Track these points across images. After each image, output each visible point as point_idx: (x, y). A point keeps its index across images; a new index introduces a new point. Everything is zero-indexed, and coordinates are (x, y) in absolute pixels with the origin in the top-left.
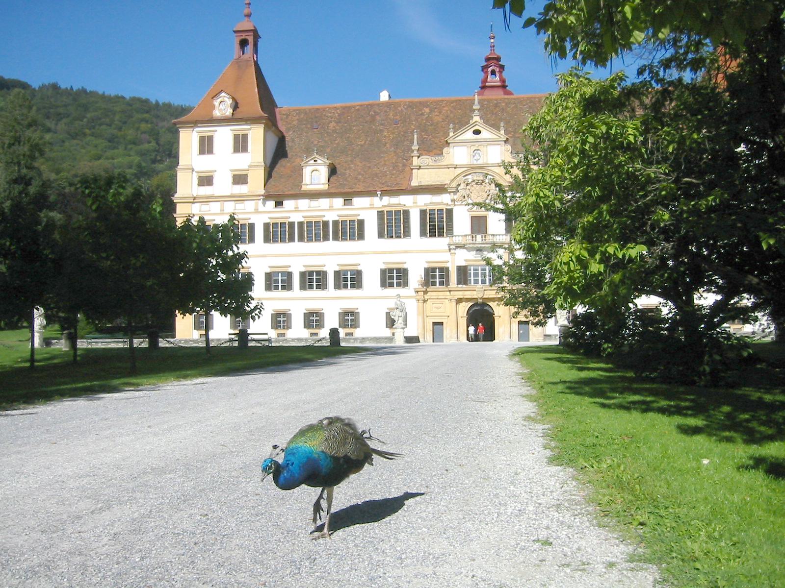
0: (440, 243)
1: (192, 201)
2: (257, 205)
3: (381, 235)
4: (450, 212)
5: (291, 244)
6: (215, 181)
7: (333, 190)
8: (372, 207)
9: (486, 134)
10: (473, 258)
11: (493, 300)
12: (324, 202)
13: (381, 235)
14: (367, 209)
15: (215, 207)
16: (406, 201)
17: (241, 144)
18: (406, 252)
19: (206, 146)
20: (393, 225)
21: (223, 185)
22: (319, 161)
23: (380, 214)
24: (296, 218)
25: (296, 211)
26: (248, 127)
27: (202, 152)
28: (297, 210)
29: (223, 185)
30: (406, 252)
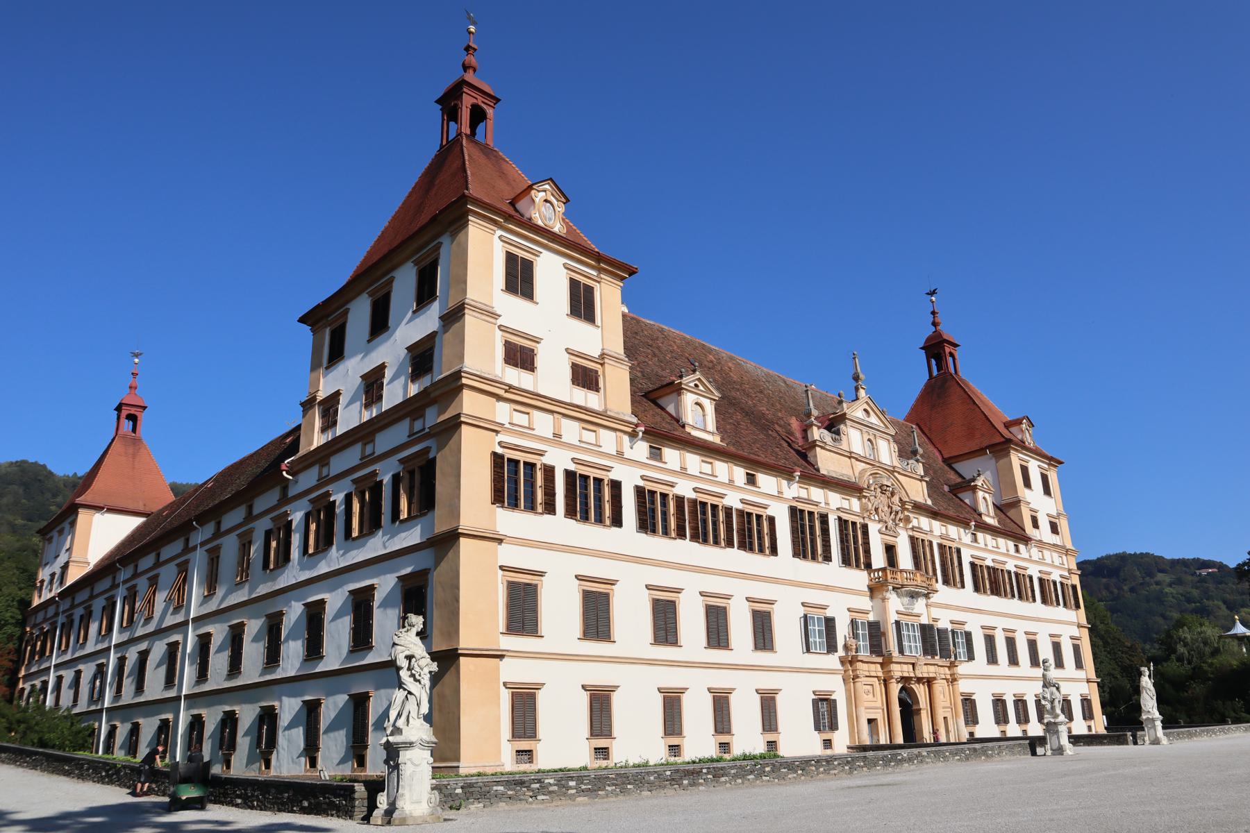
0: (860, 579)
1: (501, 392)
2: (619, 443)
3: (796, 555)
4: (865, 528)
5: (679, 541)
6: (539, 361)
7: (732, 449)
8: (779, 497)
9: (873, 419)
10: (902, 609)
11: (919, 680)
12: (722, 469)
13: (796, 554)
14: (776, 496)
15: (543, 423)
16: (817, 494)
17: (582, 304)
18: (827, 588)
19: (520, 279)
20: (808, 536)
21: (552, 377)
22: (701, 388)
23: (794, 512)
24: (685, 489)
25: (686, 475)
26: (594, 273)
27: (511, 287)
28: (683, 472)
29: (552, 377)
30: (827, 588)
